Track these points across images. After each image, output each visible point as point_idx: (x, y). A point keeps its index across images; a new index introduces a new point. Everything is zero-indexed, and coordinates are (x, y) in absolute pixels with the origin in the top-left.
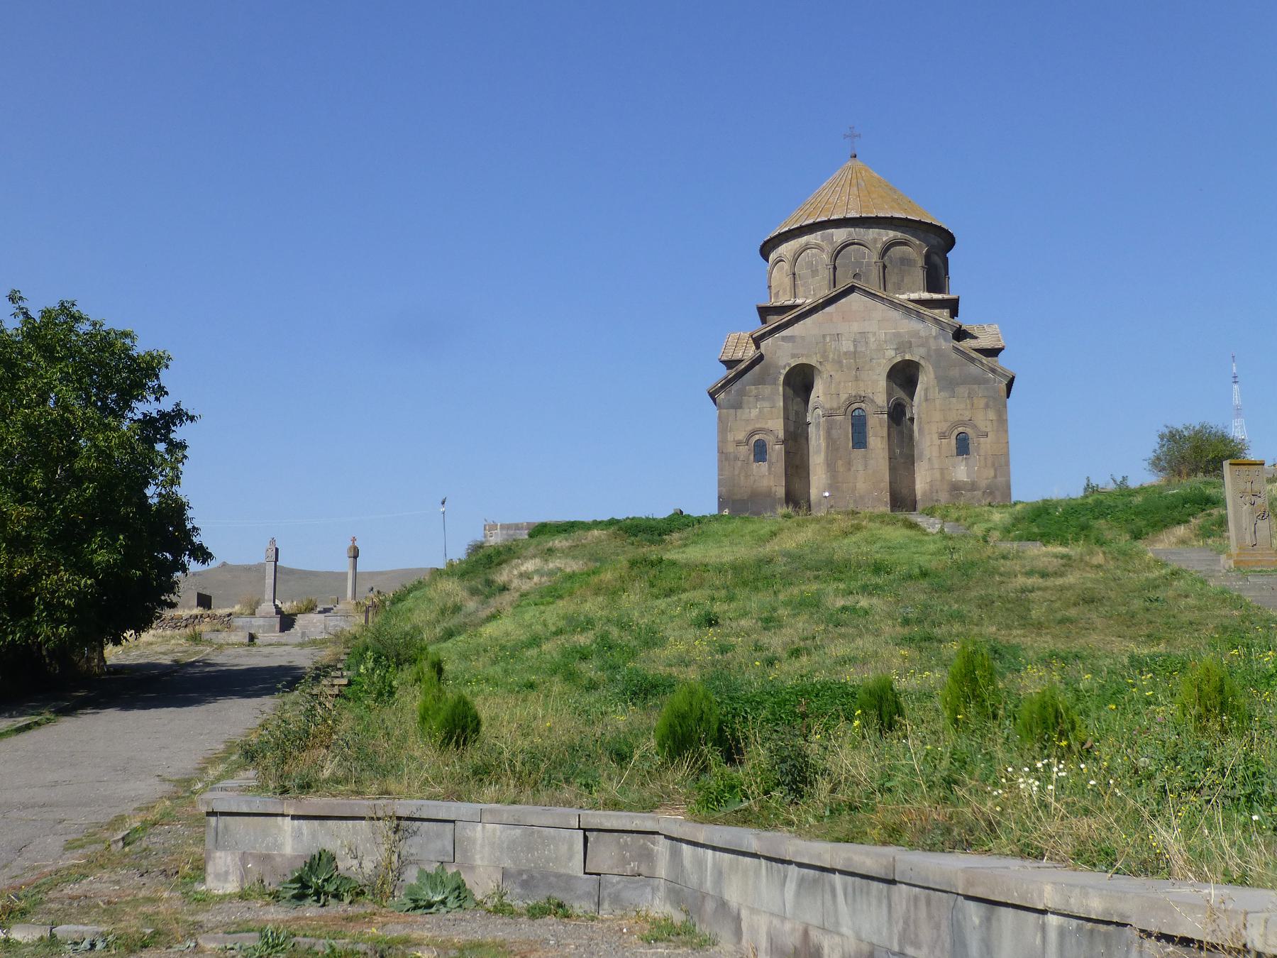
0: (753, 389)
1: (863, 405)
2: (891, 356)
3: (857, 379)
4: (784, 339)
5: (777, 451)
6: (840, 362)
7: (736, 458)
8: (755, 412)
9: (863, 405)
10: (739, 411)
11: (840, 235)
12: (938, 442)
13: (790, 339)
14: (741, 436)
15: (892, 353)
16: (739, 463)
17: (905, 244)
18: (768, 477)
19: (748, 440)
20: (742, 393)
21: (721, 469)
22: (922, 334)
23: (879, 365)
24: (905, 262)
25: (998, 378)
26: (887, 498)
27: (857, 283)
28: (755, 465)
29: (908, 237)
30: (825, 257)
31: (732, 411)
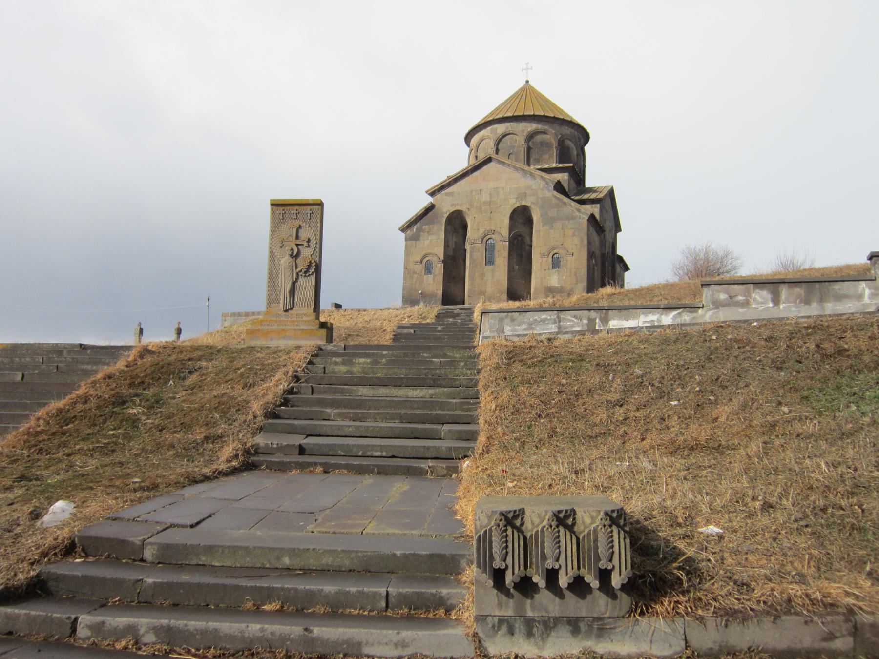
1: (493, 236)
4: (447, 194)
5: (439, 268)
6: (481, 209)
7: (414, 273)
8: (427, 242)
9: (493, 236)
11: (501, 128)
13: (451, 194)
14: (418, 258)
15: (514, 201)
16: (416, 276)
17: (544, 133)
18: (434, 283)
20: (420, 230)
21: (405, 279)
22: (534, 187)
24: (546, 145)
25: (582, 216)
27: (494, 156)
28: (425, 277)
29: (546, 127)
30: (492, 144)
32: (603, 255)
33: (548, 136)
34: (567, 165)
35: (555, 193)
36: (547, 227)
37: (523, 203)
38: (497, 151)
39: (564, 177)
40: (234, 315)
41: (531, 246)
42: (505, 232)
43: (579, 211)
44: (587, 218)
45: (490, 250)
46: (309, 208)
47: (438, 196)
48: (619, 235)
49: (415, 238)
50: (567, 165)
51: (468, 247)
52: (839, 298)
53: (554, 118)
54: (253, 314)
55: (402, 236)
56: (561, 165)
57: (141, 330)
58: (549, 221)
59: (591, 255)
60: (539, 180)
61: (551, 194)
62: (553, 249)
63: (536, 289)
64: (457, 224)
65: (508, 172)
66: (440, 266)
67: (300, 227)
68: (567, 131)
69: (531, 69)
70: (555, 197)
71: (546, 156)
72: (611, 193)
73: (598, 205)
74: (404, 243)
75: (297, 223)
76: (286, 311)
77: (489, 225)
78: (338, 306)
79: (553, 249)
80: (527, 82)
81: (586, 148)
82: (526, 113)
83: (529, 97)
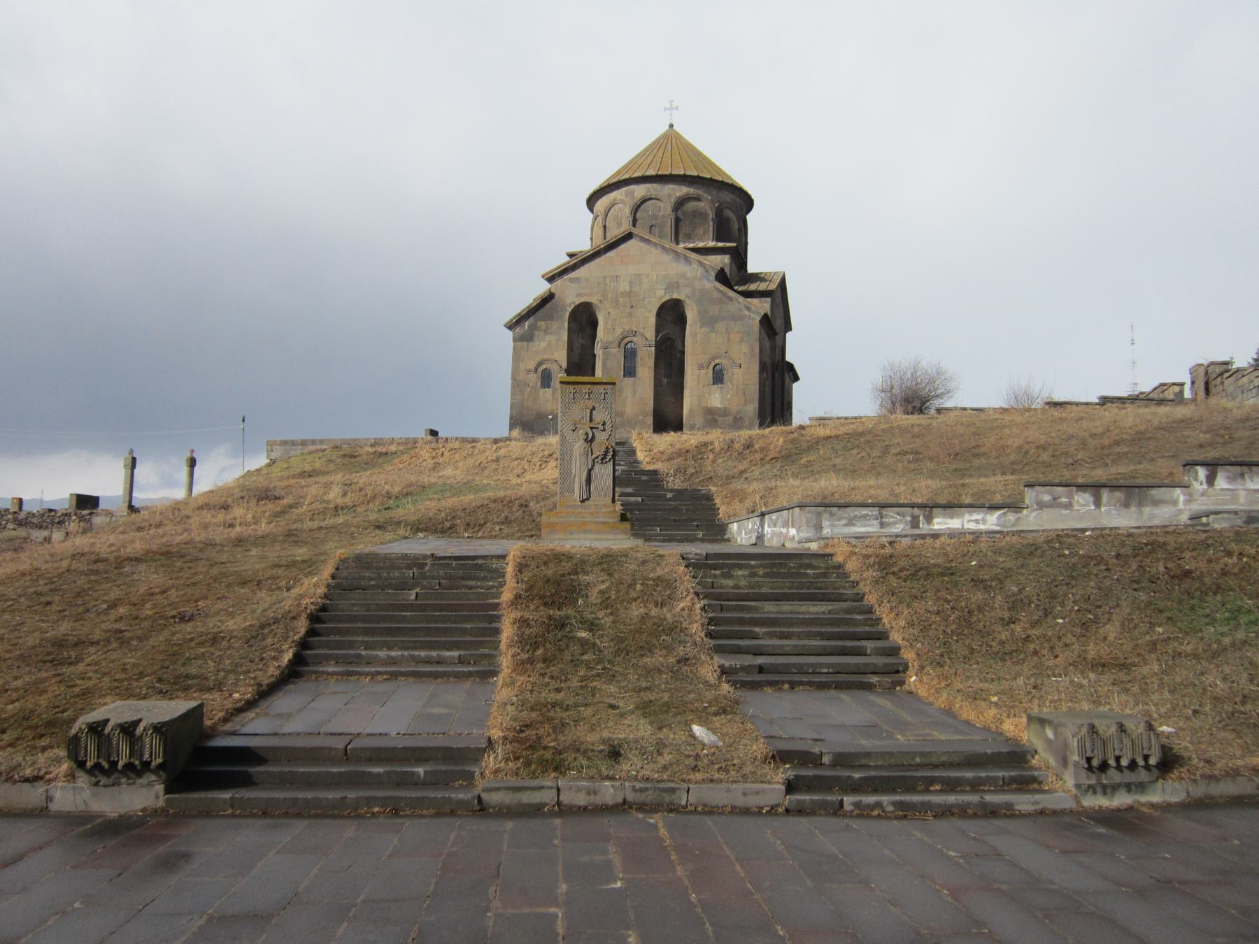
0: (542, 324)
2: (662, 296)
3: (631, 315)
4: (571, 280)
6: (617, 302)
8: (543, 345)
10: (531, 344)
11: (640, 191)
12: (697, 372)
13: (577, 280)
14: (532, 366)
15: (662, 292)
16: (528, 389)
17: (698, 199)
19: (536, 370)
20: (533, 328)
21: (513, 394)
22: (689, 275)
23: (650, 303)
24: (699, 216)
27: (634, 231)
28: (542, 391)
29: (700, 192)
30: (627, 211)
31: (525, 343)
32: (773, 363)
33: (701, 204)
34: (728, 244)
35: (718, 285)
37: (675, 296)
38: (635, 221)
39: (726, 259)
40: (285, 443)
41: (683, 352)
42: (651, 334)
43: (748, 309)
44: (758, 319)
45: (630, 356)
46: (602, 387)
47: (559, 282)
48: (788, 335)
49: (527, 338)
50: (728, 244)
51: (598, 351)
52: (1156, 503)
53: (711, 179)
54: (314, 442)
55: (510, 334)
56: (720, 244)
57: (134, 460)
58: (709, 321)
59: (763, 367)
60: (695, 266)
61: (711, 285)
62: (714, 358)
63: (691, 411)
64: (584, 321)
65: (654, 254)
67: (594, 408)
68: (727, 197)
69: (677, 108)
70: (718, 289)
71: (700, 231)
72: (783, 285)
73: (769, 300)
74: (511, 344)
75: (590, 404)
76: (583, 501)
77: (627, 323)
78: (434, 433)
79: (714, 358)
80: (671, 126)
81: (748, 217)
82: (675, 172)
83: (675, 150)
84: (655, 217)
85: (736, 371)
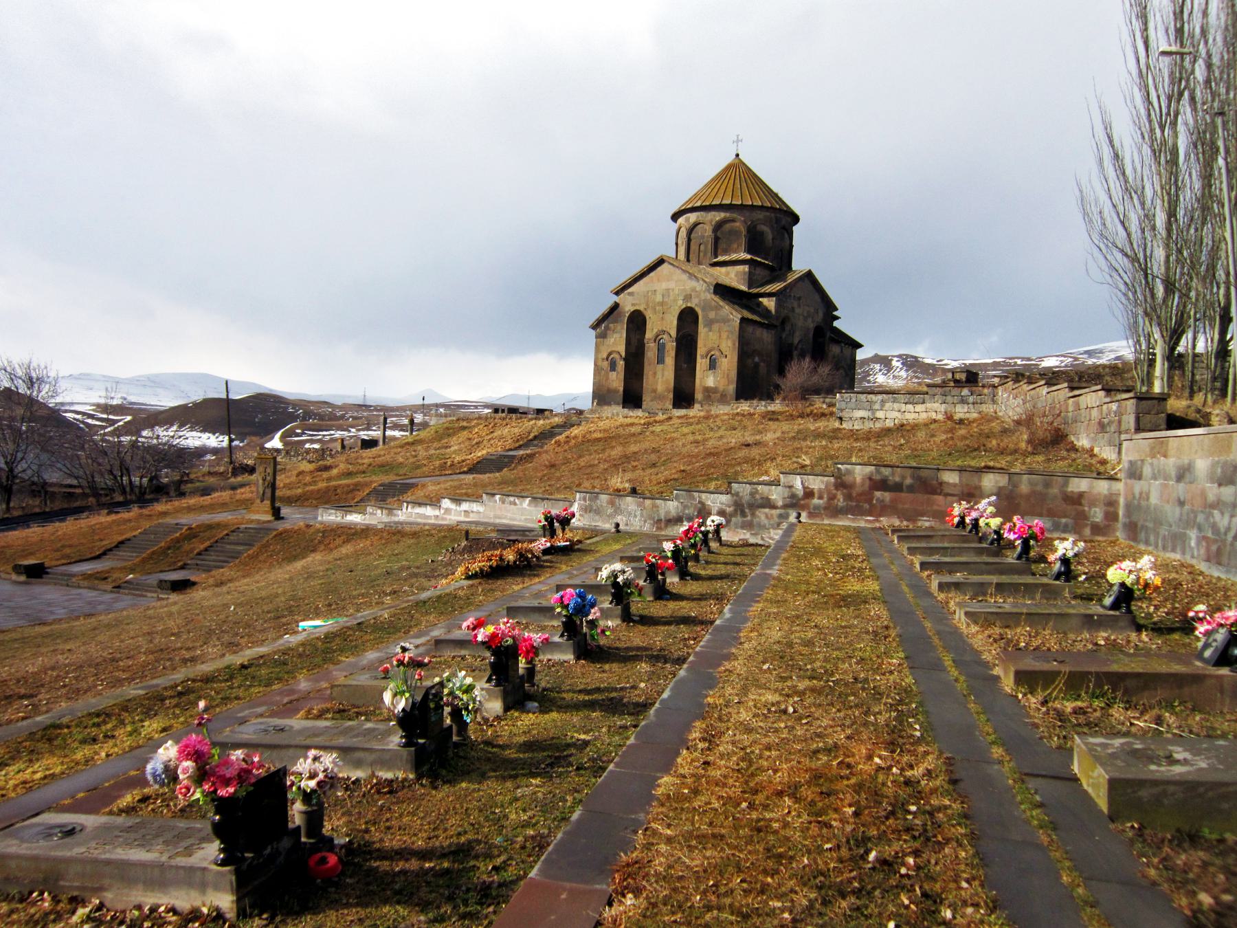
2: (681, 304)
4: (629, 294)
11: (693, 217)
13: (631, 294)
17: (733, 221)
18: (616, 380)
20: (607, 328)
21: (595, 375)
24: (734, 233)
26: (671, 396)
29: (735, 215)
33: (738, 224)
36: (706, 329)
42: (674, 333)
45: (661, 349)
55: (593, 333)
64: (637, 322)
66: (622, 363)
71: (735, 246)
84: (703, 237)
85: (724, 360)
